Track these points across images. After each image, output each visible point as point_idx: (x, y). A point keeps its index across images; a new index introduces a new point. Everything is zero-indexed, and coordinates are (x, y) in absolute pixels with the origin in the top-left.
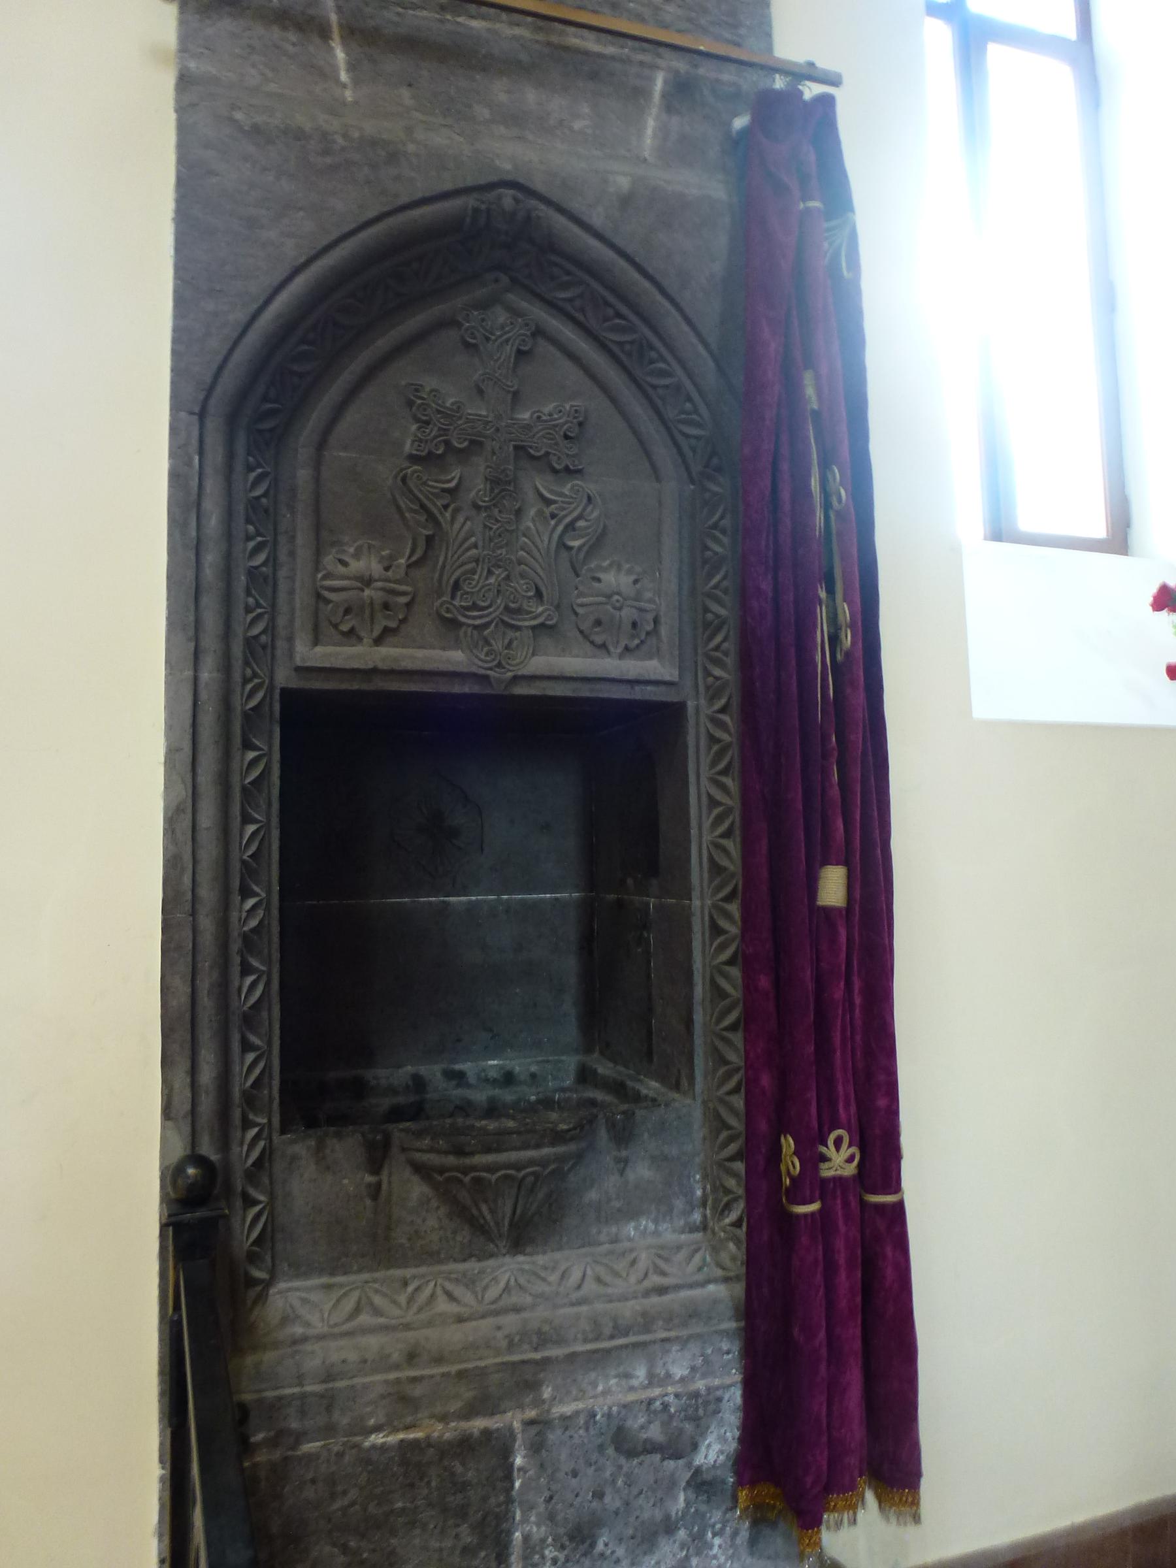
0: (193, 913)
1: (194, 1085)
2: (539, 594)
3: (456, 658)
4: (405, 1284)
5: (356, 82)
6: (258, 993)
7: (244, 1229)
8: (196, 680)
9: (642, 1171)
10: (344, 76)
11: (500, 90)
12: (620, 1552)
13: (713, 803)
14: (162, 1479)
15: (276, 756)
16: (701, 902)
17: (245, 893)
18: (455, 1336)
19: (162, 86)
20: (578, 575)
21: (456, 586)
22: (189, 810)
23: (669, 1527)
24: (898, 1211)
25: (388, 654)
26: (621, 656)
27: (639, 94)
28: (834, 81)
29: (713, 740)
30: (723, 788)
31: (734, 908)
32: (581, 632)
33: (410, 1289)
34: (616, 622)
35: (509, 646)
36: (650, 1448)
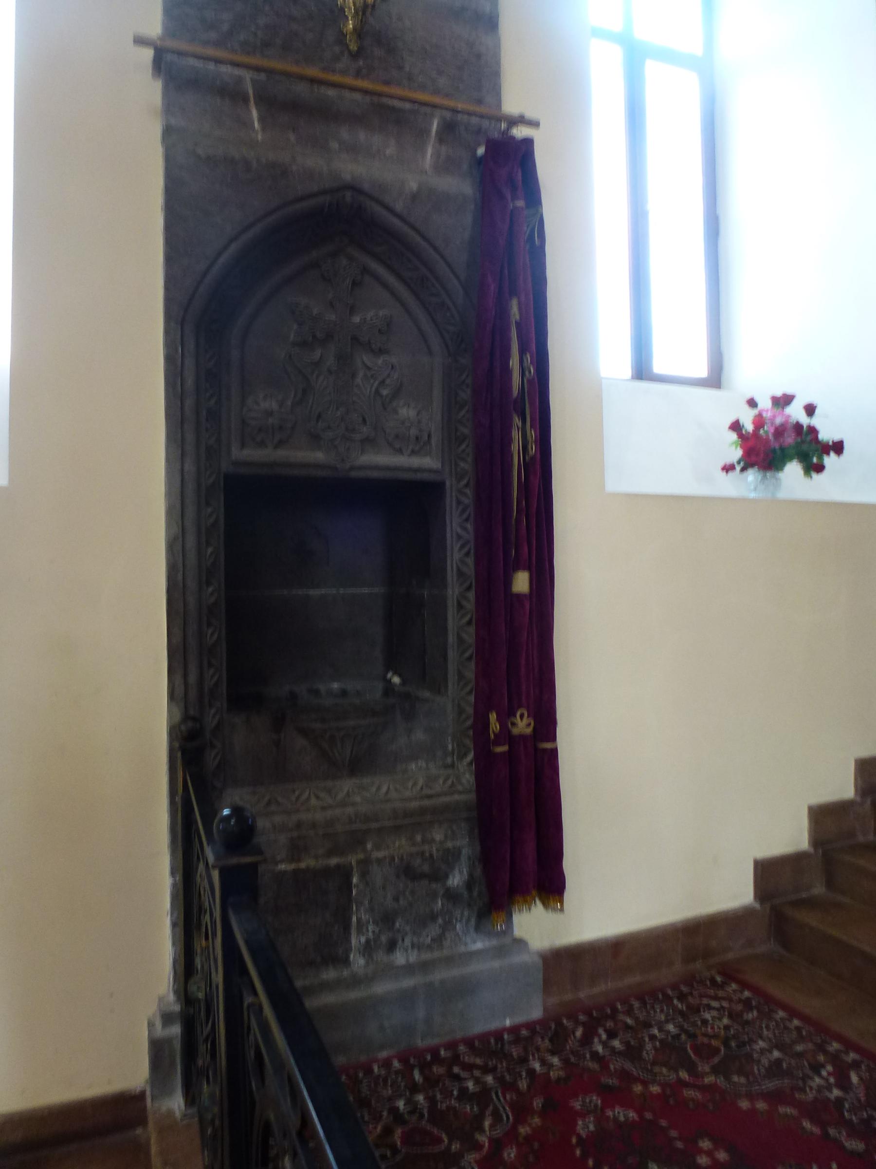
0: (184, 594)
1: (186, 684)
2: (364, 420)
3: (319, 456)
4: (294, 791)
5: (264, 129)
6: (216, 636)
7: (211, 759)
8: (182, 470)
9: (419, 735)
10: (256, 124)
11: (345, 134)
12: (408, 928)
13: (459, 537)
14: (174, 885)
15: (222, 510)
16: (453, 591)
17: (208, 583)
18: (319, 816)
19: (156, 129)
20: (385, 409)
21: (319, 416)
22: (181, 539)
23: (433, 917)
24: (554, 753)
25: (281, 454)
26: (409, 455)
27: (422, 133)
28: (535, 124)
29: (459, 502)
30: (465, 529)
31: (471, 595)
32: (388, 443)
33: (297, 793)
34: (406, 435)
35: (349, 449)
36: (423, 876)
